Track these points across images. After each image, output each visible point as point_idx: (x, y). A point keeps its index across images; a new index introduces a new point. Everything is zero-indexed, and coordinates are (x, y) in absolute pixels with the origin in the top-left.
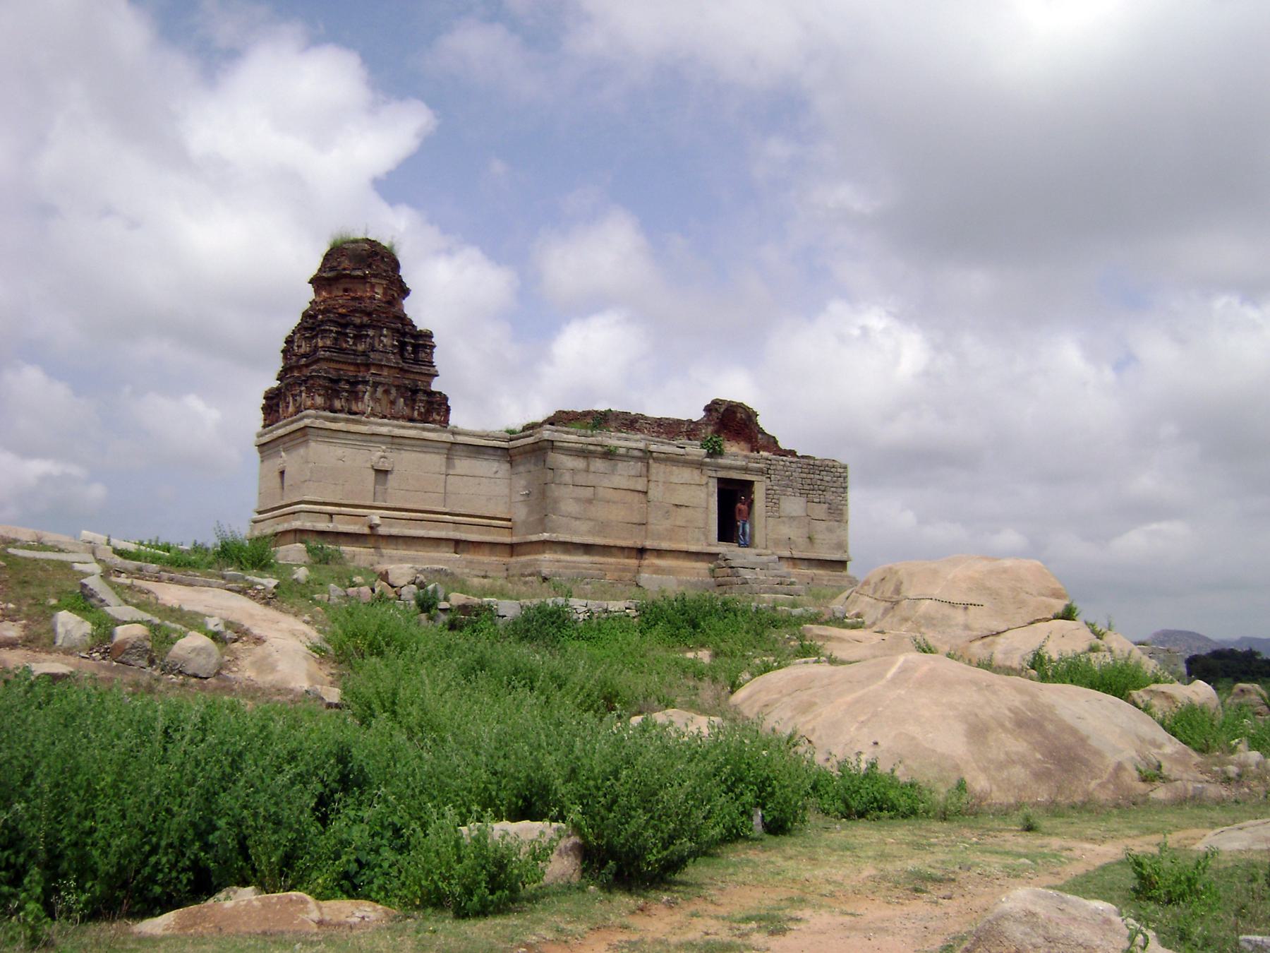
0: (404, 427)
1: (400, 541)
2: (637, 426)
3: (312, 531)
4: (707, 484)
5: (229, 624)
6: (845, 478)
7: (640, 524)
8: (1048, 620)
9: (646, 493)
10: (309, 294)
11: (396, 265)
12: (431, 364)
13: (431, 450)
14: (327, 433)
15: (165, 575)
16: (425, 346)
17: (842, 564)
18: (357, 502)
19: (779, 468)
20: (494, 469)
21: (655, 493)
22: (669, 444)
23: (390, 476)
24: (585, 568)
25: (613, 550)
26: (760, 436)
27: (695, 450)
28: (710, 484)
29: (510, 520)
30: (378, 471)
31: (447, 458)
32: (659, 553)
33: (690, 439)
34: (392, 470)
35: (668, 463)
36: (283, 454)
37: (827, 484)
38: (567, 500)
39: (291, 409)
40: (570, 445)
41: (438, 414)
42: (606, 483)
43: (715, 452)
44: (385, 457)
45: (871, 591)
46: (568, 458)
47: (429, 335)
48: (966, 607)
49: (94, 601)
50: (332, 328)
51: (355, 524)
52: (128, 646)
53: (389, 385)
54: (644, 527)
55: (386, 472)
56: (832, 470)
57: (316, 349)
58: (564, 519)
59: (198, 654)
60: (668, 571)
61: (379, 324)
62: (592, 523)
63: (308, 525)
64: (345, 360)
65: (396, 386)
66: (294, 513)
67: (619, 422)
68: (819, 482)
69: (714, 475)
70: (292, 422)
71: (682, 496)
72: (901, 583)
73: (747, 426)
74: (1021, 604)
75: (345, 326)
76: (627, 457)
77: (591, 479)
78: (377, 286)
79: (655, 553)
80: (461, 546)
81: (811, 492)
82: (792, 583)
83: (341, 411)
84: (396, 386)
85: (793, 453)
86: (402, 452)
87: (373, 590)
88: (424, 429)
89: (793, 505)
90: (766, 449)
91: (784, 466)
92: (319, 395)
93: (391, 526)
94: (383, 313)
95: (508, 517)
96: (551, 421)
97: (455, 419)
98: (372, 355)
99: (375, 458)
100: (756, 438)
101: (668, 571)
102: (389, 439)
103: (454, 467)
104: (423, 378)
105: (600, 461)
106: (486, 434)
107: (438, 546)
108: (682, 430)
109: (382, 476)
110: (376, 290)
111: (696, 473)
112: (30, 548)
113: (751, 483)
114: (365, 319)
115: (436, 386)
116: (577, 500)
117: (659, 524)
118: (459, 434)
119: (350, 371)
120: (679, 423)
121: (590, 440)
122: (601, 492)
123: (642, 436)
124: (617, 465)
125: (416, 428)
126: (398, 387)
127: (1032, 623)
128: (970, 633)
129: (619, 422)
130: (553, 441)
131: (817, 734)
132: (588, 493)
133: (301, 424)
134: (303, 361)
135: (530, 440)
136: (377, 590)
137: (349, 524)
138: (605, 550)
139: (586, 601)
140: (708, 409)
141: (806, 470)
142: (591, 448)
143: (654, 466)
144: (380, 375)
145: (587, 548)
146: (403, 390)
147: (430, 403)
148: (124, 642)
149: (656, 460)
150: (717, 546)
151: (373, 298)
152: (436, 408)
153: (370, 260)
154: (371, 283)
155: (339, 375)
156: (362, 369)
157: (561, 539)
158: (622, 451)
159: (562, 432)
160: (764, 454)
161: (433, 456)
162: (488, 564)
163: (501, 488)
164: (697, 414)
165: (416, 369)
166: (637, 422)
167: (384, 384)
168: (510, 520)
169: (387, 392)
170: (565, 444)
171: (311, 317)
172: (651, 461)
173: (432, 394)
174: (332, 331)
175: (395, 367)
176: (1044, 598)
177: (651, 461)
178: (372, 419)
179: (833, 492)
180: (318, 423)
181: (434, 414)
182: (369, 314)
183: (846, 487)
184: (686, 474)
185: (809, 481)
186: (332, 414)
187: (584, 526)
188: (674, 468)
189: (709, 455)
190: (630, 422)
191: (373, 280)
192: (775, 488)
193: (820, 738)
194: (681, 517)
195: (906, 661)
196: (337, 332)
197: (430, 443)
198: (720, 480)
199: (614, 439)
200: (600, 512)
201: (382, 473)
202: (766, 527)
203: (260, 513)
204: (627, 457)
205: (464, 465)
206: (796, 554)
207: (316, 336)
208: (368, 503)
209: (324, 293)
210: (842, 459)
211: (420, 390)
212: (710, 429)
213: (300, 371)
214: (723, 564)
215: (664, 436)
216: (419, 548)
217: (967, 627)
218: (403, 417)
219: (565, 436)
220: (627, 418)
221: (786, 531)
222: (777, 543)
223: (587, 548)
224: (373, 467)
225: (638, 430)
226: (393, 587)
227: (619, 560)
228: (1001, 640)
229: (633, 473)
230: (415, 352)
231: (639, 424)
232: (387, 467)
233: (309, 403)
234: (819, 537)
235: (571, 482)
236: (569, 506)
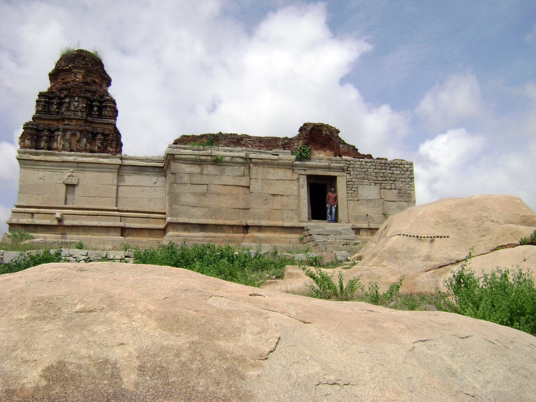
0: (86, 156)
1: (81, 229)
2: (243, 142)
6: (412, 171)
7: (244, 209)
8: (514, 246)
9: (249, 187)
13: (106, 170)
14: (31, 162)
19: (356, 166)
20: (154, 181)
21: (255, 186)
22: (266, 153)
23: (76, 188)
24: (199, 241)
25: (224, 228)
26: (341, 146)
27: (286, 156)
28: (301, 180)
30: (68, 185)
31: (118, 175)
32: (260, 228)
33: (285, 149)
34: (78, 184)
35: (265, 166)
37: (396, 176)
40: (187, 156)
41: (112, 147)
44: (73, 176)
46: (185, 165)
48: (432, 240)
50: (41, 99)
53: (75, 130)
54: (248, 210)
55: (74, 186)
56: (400, 166)
58: (184, 207)
60: (266, 241)
61: (73, 95)
62: (206, 210)
64: (49, 118)
65: (79, 131)
67: (227, 140)
68: (390, 175)
69: (303, 172)
71: (278, 188)
73: (331, 139)
74: (485, 232)
76: (232, 162)
77: (205, 179)
78: (78, 74)
79: (256, 228)
80: (127, 231)
81: (383, 182)
83: (43, 149)
84: (79, 131)
85: (370, 157)
86: (85, 172)
88: (100, 157)
90: (346, 154)
91: (361, 165)
92: (28, 139)
94: (78, 88)
95: (163, 212)
99: (65, 177)
100: (338, 147)
101: (266, 241)
102: (75, 165)
103: (124, 181)
105: (211, 167)
106: (146, 158)
107: (109, 232)
108: (279, 144)
110: (78, 77)
113: (334, 178)
116: (194, 194)
118: (127, 159)
120: (276, 139)
121: (202, 153)
122: (213, 188)
124: (224, 169)
125: (95, 156)
126: (81, 132)
127: (495, 250)
128: (429, 263)
129: (228, 140)
130: (173, 155)
132: (203, 189)
137: (41, 219)
138: (217, 228)
139: (86, 251)
140: (301, 130)
141: (379, 167)
143: (254, 169)
144: (70, 124)
145: (203, 227)
146: (85, 133)
149: (255, 164)
150: (307, 222)
154: (74, 72)
159: (181, 148)
160: (344, 157)
161: (107, 173)
162: (145, 242)
165: (100, 120)
166: (242, 140)
167: (72, 130)
170: (183, 156)
172: (251, 165)
176: (511, 225)
177: (251, 165)
178: (63, 152)
179: (402, 182)
181: (109, 147)
183: (413, 178)
184: (281, 173)
185: (382, 175)
187: (199, 212)
188: (271, 169)
191: (75, 70)
192: (354, 180)
194: (276, 203)
197: (104, 166)
198: (309, 177)
199: (220, 151)
200: (212, 202)
201: (70, 187)
204: (232, 162)
205: (130, 179)
211: (99, 133)
212: (301, 142)
215: (264, 148)
216: (94, 234)
217: (428, 258)
218: (86, 150)
219: (183, 151)
220: (235, 137)
221: (363, 210)
222: (357, 218)
223: (203, 227)
227: (228, 234)
229: (238, 174)
231: (244, 141)
232: (74, 182)
235: (189, 182)
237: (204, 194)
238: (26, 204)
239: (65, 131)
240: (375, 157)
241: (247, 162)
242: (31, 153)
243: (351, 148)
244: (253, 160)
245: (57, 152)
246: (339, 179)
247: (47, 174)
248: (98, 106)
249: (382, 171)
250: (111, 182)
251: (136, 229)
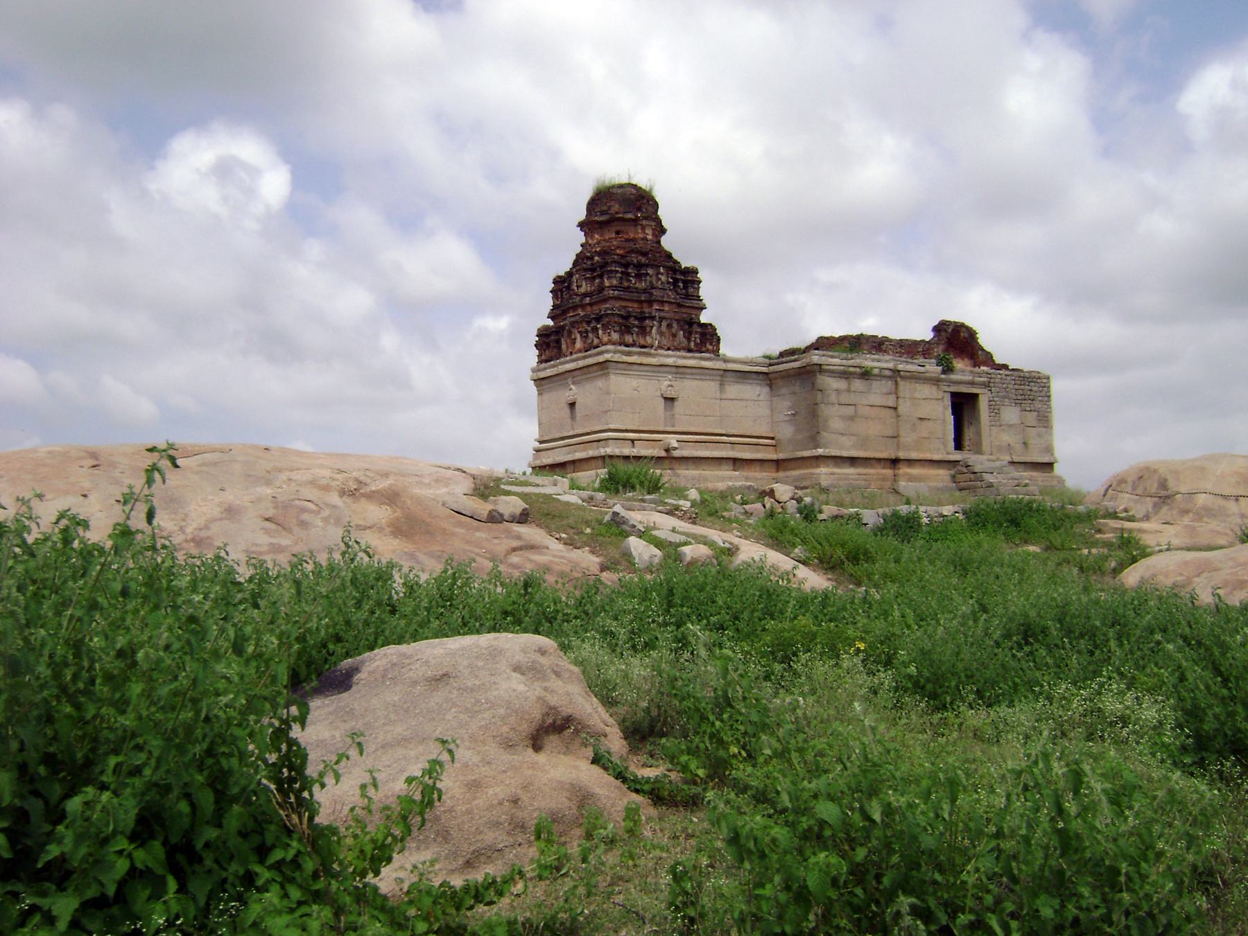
0: (685, 358)
2: (884, 347)
3: (619, 456)
6: (1049, 387)
9: (895, 408)
10: (580, 237)
12: (698, 298)
18: (685, 430)
21: (902, 409)
23: (676, 403)
29: (773, 438)
30: (666, 399)
32: (910, 462)
36: (572, 386)
38: (834, 417)
39: (579, 344)
41: (711, 344)
42: (865, 402)
43: (948, 369)
44: (671, 386)
47: (695, 272)
49: (625, 527)
51: (653, 448)
52: (700, 563)
55: (672, 400)
57: (601, 289)
62: (854, 438)
63: (617, 452)
66: (599, 441)
70: (584, 358)
71: (926, 410)
75: (626, 266)
77: (852, 398)
82: (1026, 485)
83: (633, 345)
85: (1005, 367)
87: (764, 506)
88: (701, 359)
89: (1011, 414)
90: (985, 364)
97: (724, 349)
99: (663, 388)
104: (693, 311)
107: (720, 465)
109: (669, 402)
111: (934, 387)
113: (976, 396)
114: (643, 260)
115: (704, 318)
116: (843, 417)
117: (907, 437)
119: (634, 307)
121: (851, 362)
123: (891, 357)
125: (695, 358)
132: (850, 411)
133: (601, 359)
136: (768, 506)
138: (866, 461)
142: (851, 369)
143: (901, 383)
145: (853, 461)
146: (682, 323)
147: (703, 335)
151: (645, 239)
152: (707, 338)
153: (638, 204)
155: (629, 312)
156: (645, 305)
157: (833, 454)
158: (876, 371)
160: (983, 368)
163: (764, 410)
164: (928, 335)
168: (773, 438)
169: (669, 326)
172: (899, 379)
174: (617, 272)
177: (899, 379)
178: (660, 351)
180: (617, 357)
182: (645, 254)
184: (926, 391)
185: (1021, 392)
186: (627, 349)
189: (944, 372)
190: (878, 345)
191: (644, 222)
196: (622, 273)
197: (707, 371)
198: (955, 396)
199: (869, 361)
202: (990, 435)
203: (541, 442)
204: (881, 376)
205: (734, 390)
206: (1016, 459)
208: (661, 429)
209: (596, 236)
210: (1045, 372)
212: (941, 347)
213: (583, 310)
214: (965, 470)
218: (683, 349)
221: (1006, 438)
222: (1000, 449)
223: (853, 461)
225: (885, 351)
226: (779, 503)
229: (885, 390)
230: (685, 288)
234: (1032, 442)
236: (836, 424)
237: (852, 418)
239: (661, 319)
241: (895, 374)
245: (653, 351)
246: (981, 397)
247: (642, 382)
251: (746, 460)
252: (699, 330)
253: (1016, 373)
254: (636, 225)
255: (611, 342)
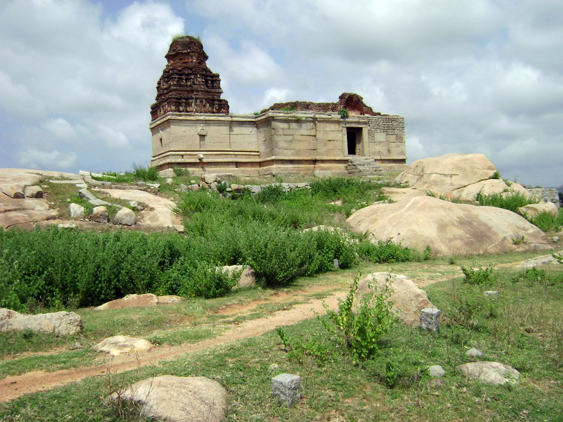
0: (210, 116)
1: (212, 164)
2: (310, 107)
3: (175, 163)
4: (342, 130)
5: (139, 204)
8: (486, 179)
9: (315, 136)
10: (165, 62)
11: (201, 47)
12: (219, 88)
13: (222, 125)
15: (113, 186)
16: (216, 80)
17: (403, 161)
19: (373, 121)
20: (250, 131)
22: (324, 114)
24: (292, 170)
26: (364, 108)
27: (336, 116)
29: (258, 152)
30: (200, 136)
31: (230, 128)
32: (323, 161)
33: (333, 111)
36: (161, 131)
38: (282, 142)
39: (162, 112)
41: (224, 109)
43: (345, 116)
45: (412, 171)
47: (218, 76)
48: (451, 176)
49: (85, 198)
51: (193, 158)
52: (99, 215)
53: (202, 99)
57: (170, 86)
59: (127, 216)
62: (293, 151)
65: (205, 99)
66: (167, 156)
68: (391, 126)
70: (163, 118)
72: (424, 167)
74: (475, 173)
75: (181, 75)
76: (306, 121)
77: (291, 132)
80: (238, 164)
82: (381, 170)
83: (183, 111)
84: (205, 99)
85: (379, 114)
87: (199, 186)
88: (219, 116)
89: (380, 136)
90: (367, 113)
91: (376, 120)
93: (208, 158)
96: (272, 108)
97: (231, 110)
98: (194, 86)
100: (363, 109)
102: (204, 122)
103: (233, 131)
107: (229, 165)
111: (337, 126)
112: (58, 179)
113: (361, 129)
114: (190, 71)
115: (222, 97)
116: (286, 141)
117: (322, 149)
118: (234, 117)
119: (185, 95)
120: (328, 105)
121: (289, 115)
123: (312, 112)
125: (215, 116)
126: (206, 99)
127: (480, 181)
130: (273, 117)
131: (376, 231)
132: (290, 138)
133: (167, 118)
134: (165, 91)
135: (264, 117)
136: (201, 185)
140: (341, 98)
141: (386, 121)
142: (290, 118)
145: (292, 162)
148: (97, 214)
149: (319, 121)
151: (192, 62)
152: (223, 106)
153: (190, 45)
155: (181, 96)
157: (280, 159)
158: (304, 119)
160: (366, 115)
163: (254, 139)
164: (336, 100)
165: (213, 90)
166: (309, 105)
168: (258, 152)
169: (201, 102)
171: (167, 72)
173: (221, 101)
174: (176, 78)
175: (204, 91)
176: (485, 170)
178: (196, 114)
180: (174, 117)
182: (191, 69)
184: (333, 127)
185: (387, 126)
186: (179, 113)
187: (289, 152)
189: (342, 118)
190: (307, 106)
191: (192, 54)
192: (372, 130)
193: (377, 233)
194: (331, 145)
195: (415, 200)
196: (178, 78)
198: (348, 129)
199: (300, 114)
200: (296, 146)
201: (202, 137)
202: (369, 147)
203: (154, 157)
204: (306, 121)
205: (237, 130)
206: (383, 158)
207: (169, 81)
208: (197, 149)
209: (171, 62)
212: (342, 106)
213: (164, 96)
214: (350, 164)
216: (221, 167)
217: (451, 184)
218: (209, 112)
219: (278, 114)
221: (378, 148)
222: (374, 153)
223: (292, 162)
224: (198, 134)
225: (310, 109)
226: (207, 183)
228: (465, 189)
229: (309, 128)
230: (212, 83)
232: (204, 133)
233: (169, 109)
234: (392, 150)
236: (282, 144)
238: (178, 149)
239: (196, 99)
240: (382, 114)
241: (314, 120)
242: (177, 115)
243: (370, 109)
244: (318, 119)
245: (193, 114)
246: (364, 129)
247: (187, 128)
248: (211, 81)
249: (387, 123)
250: (226, 133)
252: (218, 103)
253: (385, 117)
254: (189, 55)
255: (171, 111)
